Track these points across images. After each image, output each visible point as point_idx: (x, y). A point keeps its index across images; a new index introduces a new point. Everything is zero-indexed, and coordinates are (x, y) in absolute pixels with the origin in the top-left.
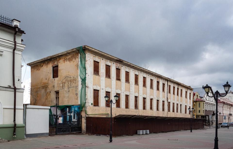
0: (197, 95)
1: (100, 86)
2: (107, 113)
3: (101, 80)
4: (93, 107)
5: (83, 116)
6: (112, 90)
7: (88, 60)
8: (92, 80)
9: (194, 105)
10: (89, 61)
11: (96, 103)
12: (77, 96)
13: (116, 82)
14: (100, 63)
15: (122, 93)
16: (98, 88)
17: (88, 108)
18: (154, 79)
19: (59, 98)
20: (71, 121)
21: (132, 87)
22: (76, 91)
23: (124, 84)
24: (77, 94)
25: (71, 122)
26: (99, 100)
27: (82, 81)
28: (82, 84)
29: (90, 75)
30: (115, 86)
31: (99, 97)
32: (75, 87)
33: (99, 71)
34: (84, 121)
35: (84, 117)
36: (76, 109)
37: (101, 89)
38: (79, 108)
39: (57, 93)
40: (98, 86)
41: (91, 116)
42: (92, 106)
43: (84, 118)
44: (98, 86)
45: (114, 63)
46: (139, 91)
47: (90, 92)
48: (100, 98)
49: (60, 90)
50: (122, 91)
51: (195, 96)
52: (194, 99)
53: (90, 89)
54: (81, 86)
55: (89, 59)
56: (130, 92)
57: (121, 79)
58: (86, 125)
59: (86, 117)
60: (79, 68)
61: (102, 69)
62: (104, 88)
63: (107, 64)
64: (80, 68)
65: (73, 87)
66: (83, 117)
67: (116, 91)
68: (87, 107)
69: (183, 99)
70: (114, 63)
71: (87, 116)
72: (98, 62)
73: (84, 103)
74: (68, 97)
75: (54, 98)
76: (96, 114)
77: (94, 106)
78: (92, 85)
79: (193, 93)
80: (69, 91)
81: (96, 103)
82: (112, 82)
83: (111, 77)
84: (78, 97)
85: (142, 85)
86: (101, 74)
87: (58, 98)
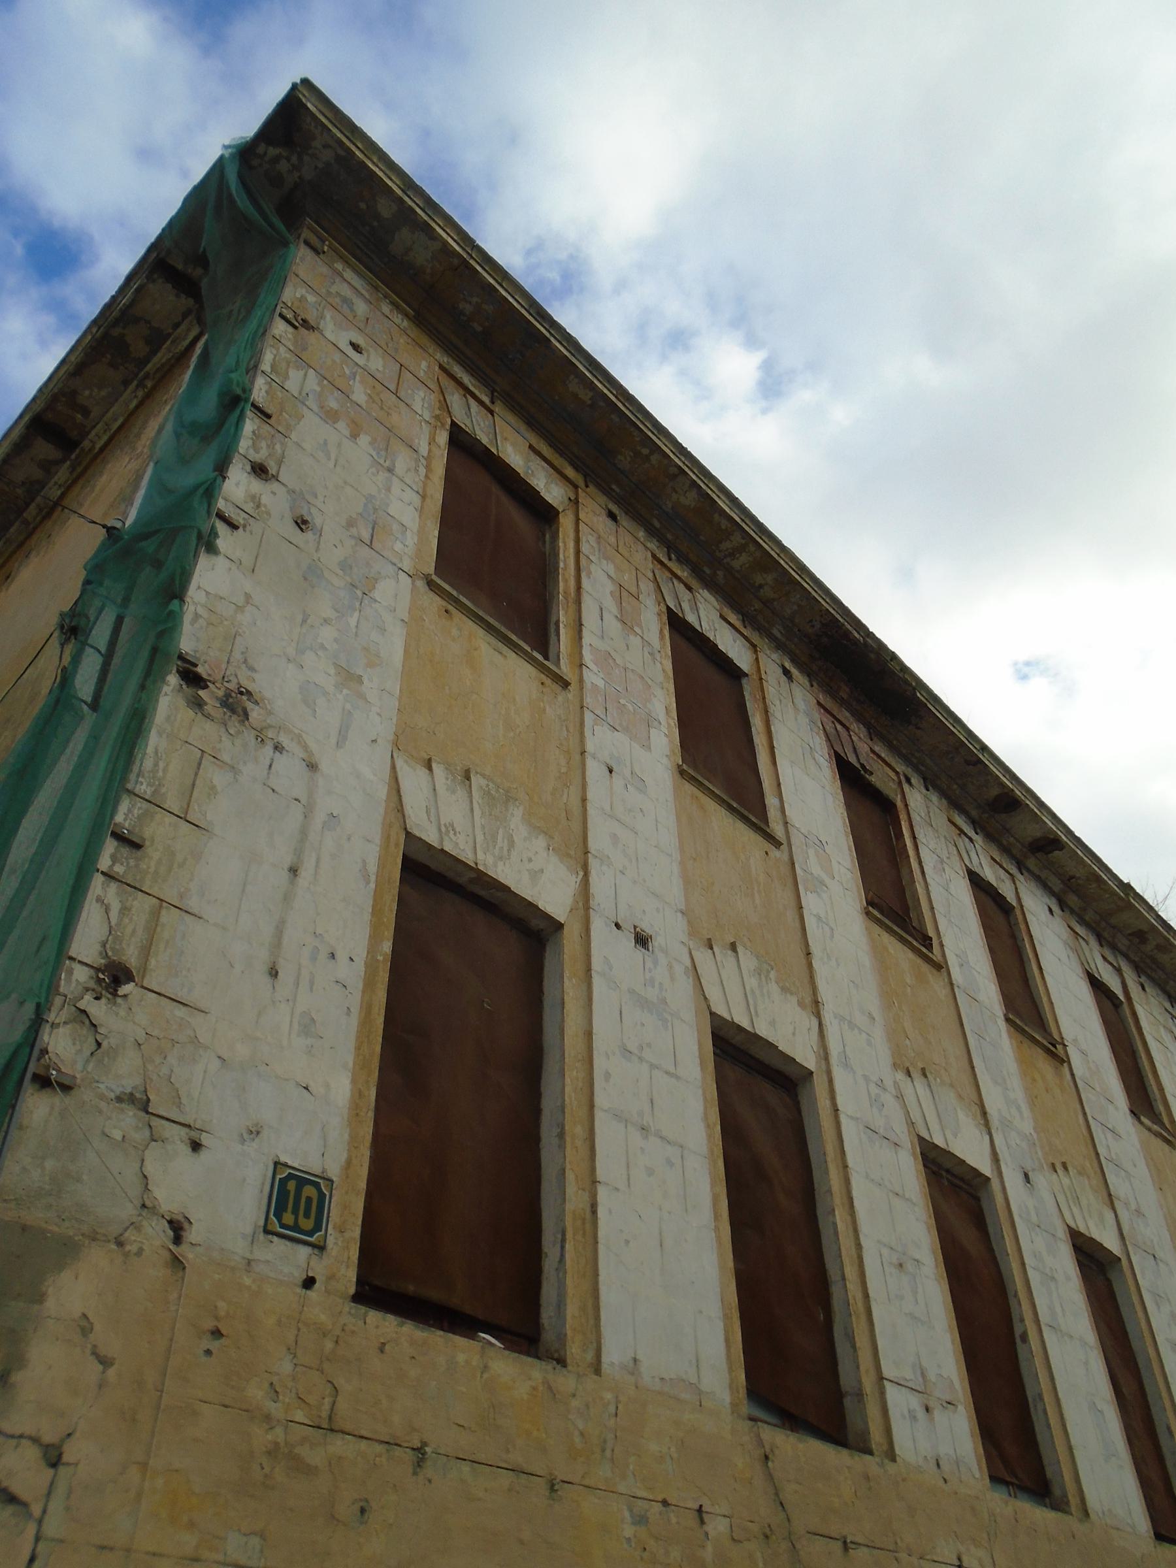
1: (581, 858)
3: (594, 770)
17: (72, 1292)
26: (560, 1161)
31: (562, 1087)
37: (599, 928)
42: (291, 1259)
53: (288, 767)
61: (613, 625)
62: (669, 931)
68: (66, 1251)
77: (373, 1292)
86: (593, 677)
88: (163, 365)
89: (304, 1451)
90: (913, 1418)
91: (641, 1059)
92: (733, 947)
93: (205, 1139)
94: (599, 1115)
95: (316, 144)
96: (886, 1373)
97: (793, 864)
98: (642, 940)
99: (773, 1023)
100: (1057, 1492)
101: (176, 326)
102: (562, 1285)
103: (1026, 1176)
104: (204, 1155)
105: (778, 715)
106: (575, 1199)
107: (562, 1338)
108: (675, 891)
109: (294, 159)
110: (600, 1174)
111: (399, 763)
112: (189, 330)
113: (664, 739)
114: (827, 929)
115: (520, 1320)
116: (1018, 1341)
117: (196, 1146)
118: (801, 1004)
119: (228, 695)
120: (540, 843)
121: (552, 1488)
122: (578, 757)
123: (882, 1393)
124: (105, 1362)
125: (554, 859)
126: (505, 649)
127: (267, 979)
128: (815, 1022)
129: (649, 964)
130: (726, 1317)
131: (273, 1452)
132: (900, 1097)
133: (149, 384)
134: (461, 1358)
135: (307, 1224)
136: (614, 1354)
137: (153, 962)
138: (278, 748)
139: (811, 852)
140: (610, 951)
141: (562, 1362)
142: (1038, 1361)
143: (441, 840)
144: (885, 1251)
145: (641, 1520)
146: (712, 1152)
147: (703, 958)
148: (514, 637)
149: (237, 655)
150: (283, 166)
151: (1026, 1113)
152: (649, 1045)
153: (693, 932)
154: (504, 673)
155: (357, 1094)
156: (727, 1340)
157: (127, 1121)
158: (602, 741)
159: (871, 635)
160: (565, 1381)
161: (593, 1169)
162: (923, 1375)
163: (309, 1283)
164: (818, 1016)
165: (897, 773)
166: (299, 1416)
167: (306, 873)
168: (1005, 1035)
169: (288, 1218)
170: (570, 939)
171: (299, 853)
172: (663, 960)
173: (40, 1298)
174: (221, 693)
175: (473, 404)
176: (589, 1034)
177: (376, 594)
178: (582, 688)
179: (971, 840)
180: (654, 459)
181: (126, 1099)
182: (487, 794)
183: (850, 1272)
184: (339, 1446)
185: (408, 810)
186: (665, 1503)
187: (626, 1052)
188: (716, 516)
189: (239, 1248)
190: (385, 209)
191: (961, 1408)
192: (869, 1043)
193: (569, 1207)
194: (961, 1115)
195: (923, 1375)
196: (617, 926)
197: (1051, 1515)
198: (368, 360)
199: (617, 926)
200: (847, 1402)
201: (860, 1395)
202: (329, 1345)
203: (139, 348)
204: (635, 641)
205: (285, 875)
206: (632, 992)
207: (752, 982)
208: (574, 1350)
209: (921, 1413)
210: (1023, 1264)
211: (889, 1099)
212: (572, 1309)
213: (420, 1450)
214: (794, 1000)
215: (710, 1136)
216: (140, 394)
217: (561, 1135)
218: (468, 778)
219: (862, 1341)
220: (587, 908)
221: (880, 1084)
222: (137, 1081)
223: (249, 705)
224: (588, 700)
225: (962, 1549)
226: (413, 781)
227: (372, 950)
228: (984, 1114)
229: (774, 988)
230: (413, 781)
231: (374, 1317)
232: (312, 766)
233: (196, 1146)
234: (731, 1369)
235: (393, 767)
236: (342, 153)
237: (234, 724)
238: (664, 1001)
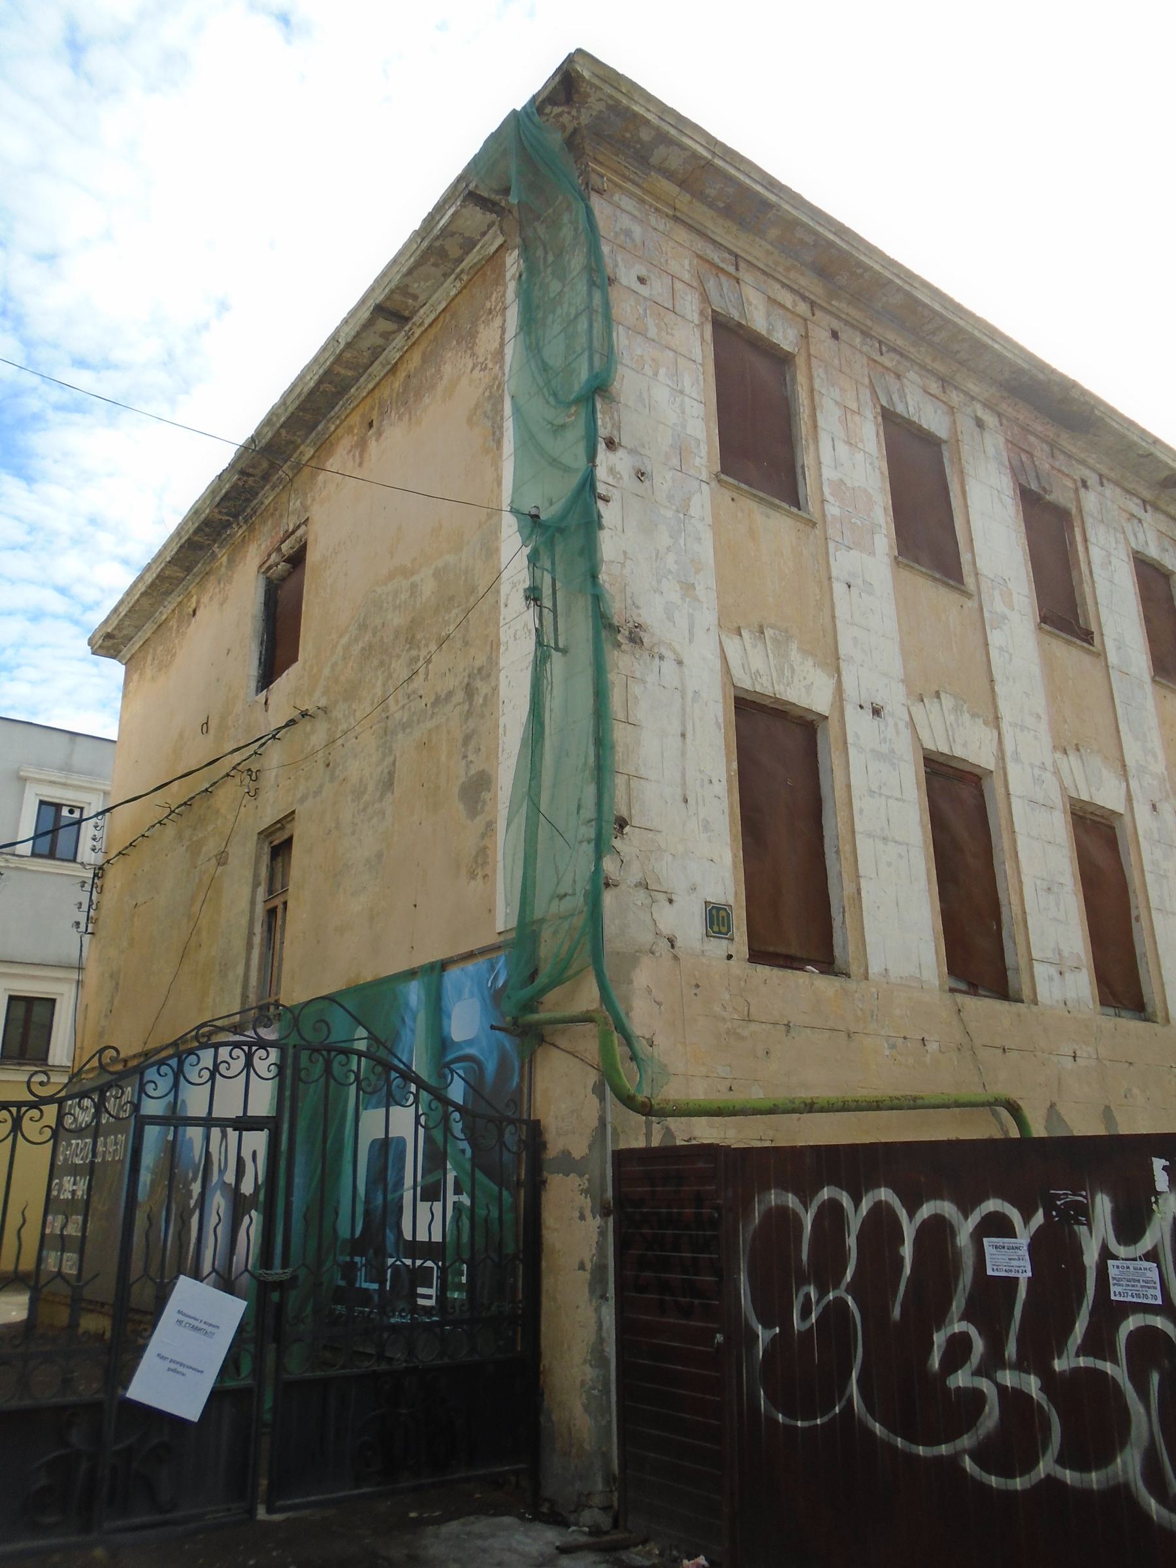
1: (833, 663)
2: (974, 1092)
3: (839, 588)
4: (740, 967)
6: (1009, 748)
8: (706, 551)
10: (643, 290)
11: (791, 907)
12: (473, 812)
13: (1049, 664)
14: (800, 361)
16: (807, 689)
17: (642, 976)
20: (390, 1236)
22: (467, 739)
23: (1150, 704)
24: (477, 789)
25: (381, 1253)
27: (533, 559)
28: (547, 602)
30: (1039, 702)
32: (460, 696)
33: (807, 459)
34: (576, 1233)
35: (579, 1149)
36: (466, 1022)
37: (850, 712)
39: (279, 847)
40: (795, 655)
41: (706, 1132)
42: (719, 947)
43: (574, 1181)
44: (795, 655)
45: (990, 420)
47: (675, 728)
48: (842, 829)
49: (303, 800)
50: (1133, 784)
53: (669, 666)
54: (529, 617)
57: (1094, 628)
58: (625, 1327)
59: (622, 1158)
60: (509, 425)
61: (842, 449)
62: (894, 697)
63: (900, 409)
64: (517, 410)
65: (437, 702)
66: (568, 1165)
67: (1057, 772)
70: (980, 424)
71: (637, 1135)
72: (781, 360)
73: (578, 901)
74: (379, 856)
75: (244, 921)
76: (805, 1095)
77: (757, 956)
78: (708, 616)
80: (388, 783)
81: (791, 907)
82: (996, 638)
83: (969, 580)
84: (490, 826)
86: (833, 510)
87: (285, 903)
88: (475, 264)
89: (739, 1031)
90: (1051, 979)
91: (880, 795)
92: (937, 695)
93: (674, 897)
94: (858, 837)
95: (591, 100)
96: (1034, 957)
97: (982, 609)
98: (877, 712)
99: (965, 745)
100: (1149, 1009)
101: (484, 234)
102: (845, 935)
103: (1154, 807)
104: (675, 904)
105: (971, 472)
106: (849, 889)
107: (847, 964)
108: (897, 670)
109: (574, 112)
110: (861, 872)
111: (723, 638)
112: (494, 238)
113: (884, 540)
114: (1006, 655)
115: (825, 960)
116: (1133, 921)
117: (671, 901)
118: (986, 723)
119: (631, 633)
120: (810, 662)
121: (849, 1036)
122: (826, 582)
123: (1031, 968)
124: (659, 1004)
125: (819, 671)
126: (769, 511)
127: (683, 805)
128: (995, 733)
129: (882, 728)
130: (936, 939)
131: (728, 1032)
132: (1057, 772)
133: (465, 277)
134: (801, 981)
135: (724, 930)
136: (875, 969)
137: (633, 812)
138: (661, 658)
139: (996, 593)
140: (858, 725)
141: (848, 975)
142: (1146, 934)
143: (754, 685)
144: (1039, 882)
145: (893, 1047)
146: (925, 841)
147: (917, 710)
148: (777, 502)
149: (629, 601)
150: (566, 119)
151: (1161, 755)
152: (885, 784)
153: (909, 694)
154: (774, 527)
155: (735, 856)
156: (937, 953)
157: (641, 896)
158: (843, 562)
159: (1053, 371)
160: (851, 985)
161: (857, 869)
162: (1060, 954)
163: (730, 957)
164: (998, 728)
165: (1075, 481)
166: (736, 1017)
167: (689, 735)
168: (1150, 697)
169: (716, 928)
170: (833, 724)
171: (683, 723)
172: (890, 721)
173: (631, 982)
174: (627, 633)
175: (723, 279)
176: (849, 786)
177: (692, 512)
178: (825, 522)
179: (1140, 521)
180: (866, 276)
181: (639, 885)
182: (775, 640)
183: (1014, 899)
184: (754, 1027)
185: (733, 671)
186: (905, 1038)
187: (871, 792)
188: (920, 308)
189: (698, 946)
190: (645, 135)
191: (1084, 971)
192: (1036, 738)
193: (846, 893)
194: (1105, 772)
195: (1060, 954)
196: (861, 707)
197: (1141, 1025)
198: (651, 289)
199: (861, 707)
200: (1009, 973)
201: (1017, 970)
202: (743, 984)
203: (454, 251)
204: (859, 457)
205: (679, 739)
206: (872, 751)
207: (951, 718)
208: (854, 969)
209: (1056, 976)
210: (1143, 870)
211: (1048, 776)
212: (851, 948)
213: (788, 1025)
214: (980, 721)
215: (924, 834)
216: (458, 284)
217: (838, 852)
218: (763, 633)
219: (1020, 939)
220: (841, 699)
221: (1043, 767)
222: (641, 875)
223: (642, 634)
224: (830, 531)
225: (1076, 1047)
226: (733, 647)
227: (728, 771)
228: (1124, 766)
229: (966, 716)
230: (733, 647)
231: (759, 967)
232: (680, 663)
233: (671, 901)
234: (939, 966)
235: (720, 642)
236: (610, 102)
237: (638, 652)
238: (893, 751)
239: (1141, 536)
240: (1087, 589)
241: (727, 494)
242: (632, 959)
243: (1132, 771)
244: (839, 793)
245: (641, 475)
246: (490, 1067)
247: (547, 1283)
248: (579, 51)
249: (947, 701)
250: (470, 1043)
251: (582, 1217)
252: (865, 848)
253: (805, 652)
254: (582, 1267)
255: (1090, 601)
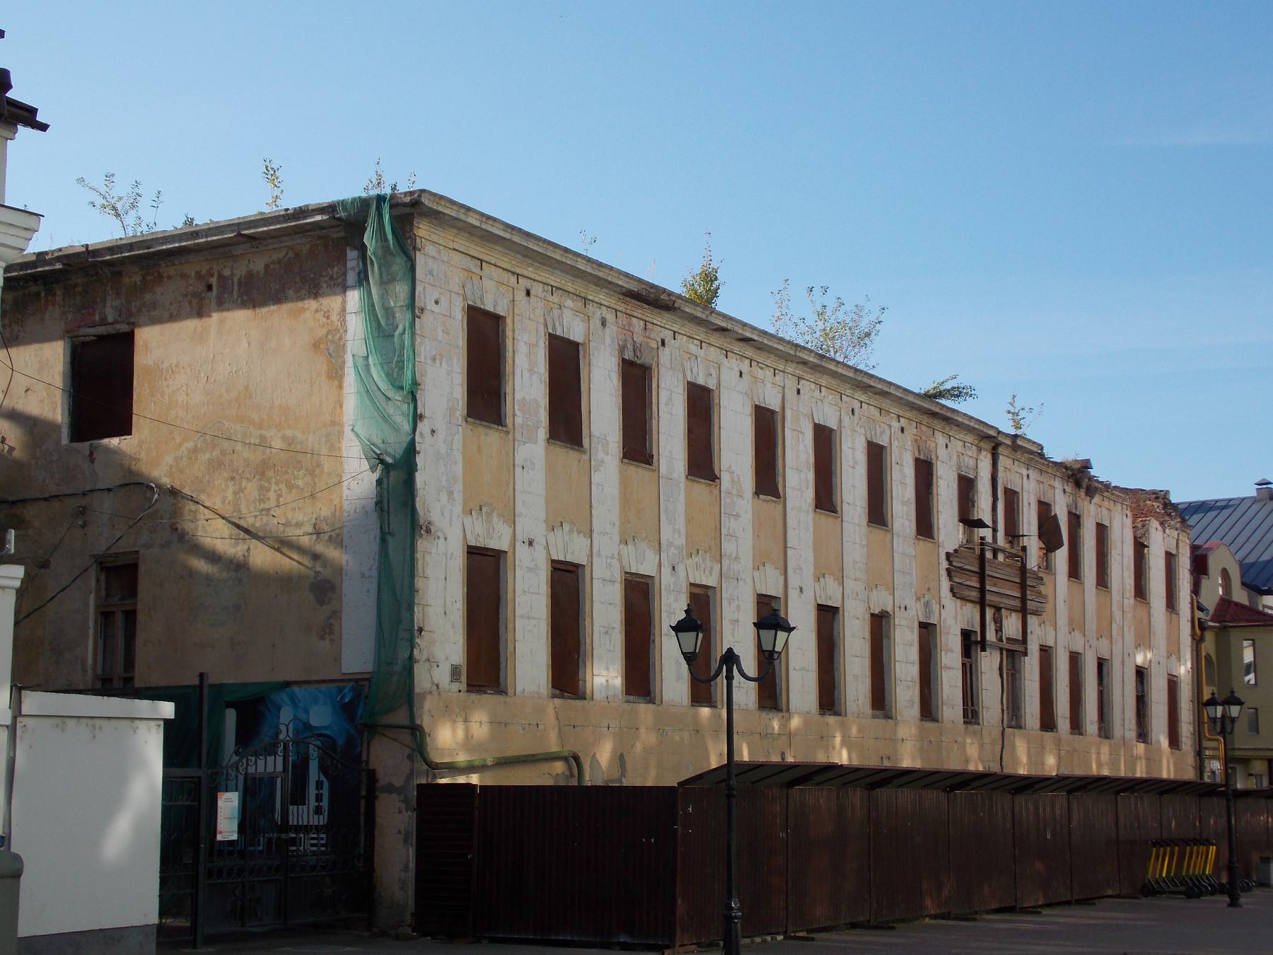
0: (1225, 574)
3: (518, 470)
5: (383, 779)
7: (430, 306)
8: (458, 469)
9: (1208, 657)
13: (624, 484)
15: (666, 570)
16: (498, 540)
17: (427, 705)
18: (895, 443)
19: (141, 617)
21: (738, 516)
29: (441, 426)
30: (615, 516)
35: (398, 782)
36: (321, 716)
37: (518, 544)
38: (347, 710)
42: (455, 687)
44: (495, 519)
46: (790, 552)
51: (1205, 583)
52: (1201, 609)
55: (436, 296)
56: (726, 562)
57: (655, 453)
61: (526, 374)
63: (559, 333)
66: (390, 789)
67: (620, 559)
69: (1117, 614)
70: (604, 323)
78: (458, 509)
79: (1194, 548)
82: (596, 478)
83: (586, 442)
85: (810, 494)
86: (519, 420)
87: (131, 616)
113: (543, 433)
132: (620, 559)
136: (519, 689)
140: (522, 553)
160: (508, 700)
170: (510, 556)
183: (588, 641)
207: (567, 538)
230: (468, 521)
239: (695, 370)
240: (654, 422)
241: (470, 427)
242: (423, 696)
243: (664, 547)
244: (510, 595)
245: (433, 431)
246: (341, 741)
247: (378, 841)
248: (423, 191)
249: (566, 527)
250: (326, 728)
251: (400, 812)
252: (519, 623)
253: (500, 516)
254: (399, 832)
255: (655, 432)
